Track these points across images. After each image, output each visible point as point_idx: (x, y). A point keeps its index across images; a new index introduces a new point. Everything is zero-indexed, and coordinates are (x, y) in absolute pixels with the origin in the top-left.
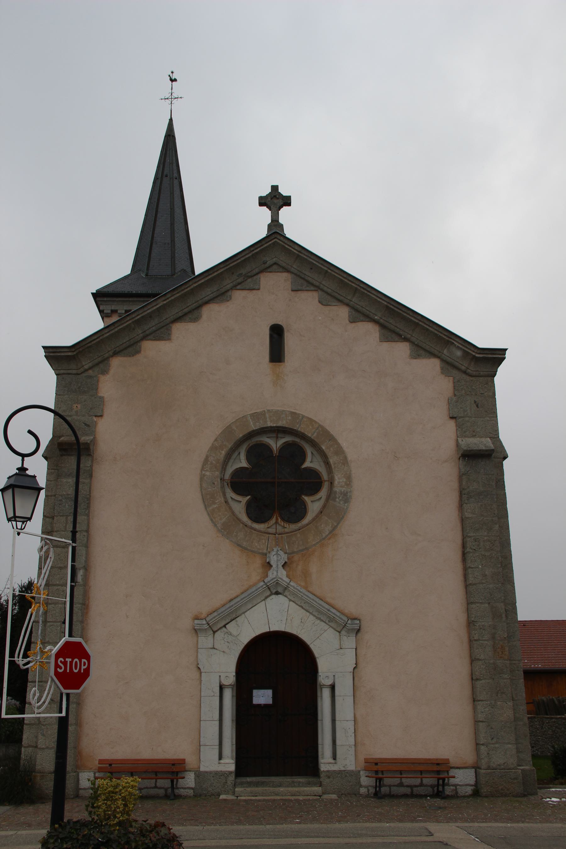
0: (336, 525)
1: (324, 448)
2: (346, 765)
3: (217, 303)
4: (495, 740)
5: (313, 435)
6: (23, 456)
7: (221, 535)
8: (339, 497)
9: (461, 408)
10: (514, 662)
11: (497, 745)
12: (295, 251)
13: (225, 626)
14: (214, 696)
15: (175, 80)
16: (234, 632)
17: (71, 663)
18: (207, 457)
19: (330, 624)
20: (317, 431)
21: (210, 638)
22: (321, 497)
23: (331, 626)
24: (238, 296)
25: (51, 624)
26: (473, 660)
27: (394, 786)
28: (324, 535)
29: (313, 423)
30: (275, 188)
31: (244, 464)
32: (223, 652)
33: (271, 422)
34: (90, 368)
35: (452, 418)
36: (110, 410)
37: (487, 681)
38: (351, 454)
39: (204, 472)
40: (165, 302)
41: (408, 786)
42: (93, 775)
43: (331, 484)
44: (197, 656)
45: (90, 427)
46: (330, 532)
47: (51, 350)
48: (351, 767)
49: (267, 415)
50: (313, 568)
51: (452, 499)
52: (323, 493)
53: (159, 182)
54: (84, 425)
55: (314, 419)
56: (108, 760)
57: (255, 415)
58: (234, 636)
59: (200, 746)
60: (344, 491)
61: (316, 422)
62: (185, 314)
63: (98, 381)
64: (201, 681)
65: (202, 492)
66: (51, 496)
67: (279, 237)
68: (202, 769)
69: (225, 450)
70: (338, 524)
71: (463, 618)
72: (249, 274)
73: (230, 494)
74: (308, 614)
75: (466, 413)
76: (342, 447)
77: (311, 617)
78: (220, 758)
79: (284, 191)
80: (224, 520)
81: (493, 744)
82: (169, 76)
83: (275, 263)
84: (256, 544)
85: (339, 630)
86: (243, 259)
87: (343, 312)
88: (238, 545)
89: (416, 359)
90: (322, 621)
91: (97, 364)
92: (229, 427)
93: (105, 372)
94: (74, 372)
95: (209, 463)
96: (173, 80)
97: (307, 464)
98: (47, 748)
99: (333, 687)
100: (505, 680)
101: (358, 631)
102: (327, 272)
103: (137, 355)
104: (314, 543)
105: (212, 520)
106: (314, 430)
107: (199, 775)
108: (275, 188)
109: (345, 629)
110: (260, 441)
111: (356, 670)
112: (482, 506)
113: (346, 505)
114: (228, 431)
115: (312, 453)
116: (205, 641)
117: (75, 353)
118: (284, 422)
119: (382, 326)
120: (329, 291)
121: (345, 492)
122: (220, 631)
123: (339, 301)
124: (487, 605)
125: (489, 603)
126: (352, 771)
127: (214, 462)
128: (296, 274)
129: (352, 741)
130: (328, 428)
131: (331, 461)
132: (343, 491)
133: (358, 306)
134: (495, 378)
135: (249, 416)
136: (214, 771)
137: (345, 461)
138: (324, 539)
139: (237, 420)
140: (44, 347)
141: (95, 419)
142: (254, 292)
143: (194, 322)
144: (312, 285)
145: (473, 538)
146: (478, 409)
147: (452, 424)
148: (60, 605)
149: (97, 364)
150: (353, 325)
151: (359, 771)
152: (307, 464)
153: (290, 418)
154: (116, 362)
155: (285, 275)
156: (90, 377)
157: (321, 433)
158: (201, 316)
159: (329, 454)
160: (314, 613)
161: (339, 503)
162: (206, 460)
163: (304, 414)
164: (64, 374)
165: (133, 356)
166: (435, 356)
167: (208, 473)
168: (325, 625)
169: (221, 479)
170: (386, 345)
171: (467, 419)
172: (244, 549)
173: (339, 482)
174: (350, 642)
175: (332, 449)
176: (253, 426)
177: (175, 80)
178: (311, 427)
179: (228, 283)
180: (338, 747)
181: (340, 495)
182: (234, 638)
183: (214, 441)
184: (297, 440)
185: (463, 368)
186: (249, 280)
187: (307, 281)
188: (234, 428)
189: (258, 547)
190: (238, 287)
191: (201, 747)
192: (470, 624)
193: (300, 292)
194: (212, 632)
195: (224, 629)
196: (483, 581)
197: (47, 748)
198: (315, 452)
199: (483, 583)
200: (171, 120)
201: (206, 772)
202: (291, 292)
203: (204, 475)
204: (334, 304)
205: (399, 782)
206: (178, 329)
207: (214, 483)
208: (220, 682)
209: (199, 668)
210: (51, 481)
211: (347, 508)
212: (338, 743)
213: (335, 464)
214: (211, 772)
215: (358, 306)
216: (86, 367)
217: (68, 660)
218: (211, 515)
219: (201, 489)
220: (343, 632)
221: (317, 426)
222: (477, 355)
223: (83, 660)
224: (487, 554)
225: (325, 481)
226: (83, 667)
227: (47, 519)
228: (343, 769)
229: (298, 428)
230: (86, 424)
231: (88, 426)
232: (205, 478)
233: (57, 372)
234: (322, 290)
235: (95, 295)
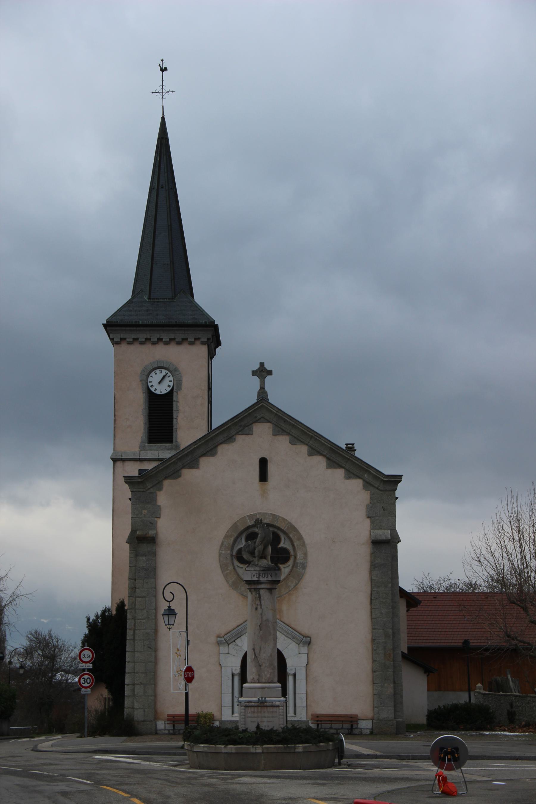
1: (291, 536)
2: (301, 717)
3: (227, 444)
4: (382, 705)
5: (285, 528)
6: (169, 602)
9: (374, 511)
10: (397, 662)
11: (383, 708)
12: (274, 411)
13: (234, 641)
14: (229, 680)
15: (166, 69)
16: (240, 645)
17: (189, 673)
19: (294, 640)
21: (226, 647)
22: (289, 565)
23: (294, 641)
24: (240, 439)
25: (138, 641)
26: (374, 661)
27: (328, 729)
28: (291, 589)
30: (262, 364)
32: (234, 655)
34: (151, 487)
35: (368, 517)
37: (381, 673)
38: (307, 540)
39: (221, 551)
40: (195, 446)
41: (335, 729)
42: (164, 723)
43: (295, 557)
44: (219, 658)
45: (153, 525)
46: (294, 587)
47: (128, 478)
48: (304, 718)
50: (284, 608)
52: (291, 562)
53: (154, 192)
54: (149, 523)
56: (172, 715)
57: (250, 516)
58: (239, 646)
59: (222, 707)
60: (303, 562)
62: (208, 452)
63: (156, 496)
64: (221, 671)
65: (220, 563)
66: (133, 566)
67: (264, 402)
68: (223, 719)
69: (233, 538)
70: (299, 582)
71: (369, 637)
72: (246, 425)
74: (281, 634)
75: (376, 514)
76: (301, 536)
77: (283, 636)
78: (233, 713)
79: (268, 367)
80: (233, 579)
81: (381, 707)
82: (159, 65)
83: (262, 417)
85: (298, 643)
86: (242, 417)
87: (304, 449)
88: (242, 595)
89: (348, 479)
90: (289, 638)
91: (156, 485)
92: (235, 523)
93: (160, 489)
94: (142, 490)
95: (224, 546)
96: (164, 70)
97: (281, 545)
98: (140, 708)
99: (294, 675)
100: (390, 673)
101: (309, 644)
102: (294, 425)
103: (179, 478)
104: (285, 593)
105: (226, 580)
107: (221, 722)
108: (262, 364)
109: (301, 642)
110: (254, 531)
111: (307, 666)
112: (382, 572)
113: (304, 570)
114: (235, 526)
115: (284, 538)
116: (224, 649)
117: (142, 480)
118: (268, 520)
119: (328, 459)
120: (296, 436)
121: (303, 563)
122: (231, 644)
123: (302, 442)
124: (382, 630)
125: (383, 629)
126: (305, 721)
127: (227, 545)
128: (275, 425)
129: (304, 704)
130: (294, 524)
131: (295, 544)
132: (302, 562)
133: (313, 446)
134: (396, 492)
135: (247, 516)
136: (230, 720)
137: (304, 544)
139: (240, 519)
140: (123, 477)
141: (156, 519)
142: (250, 436)
143: (213, 456)
144: (286, 432)
145: (376, 591)
146: (384, 512)
147: (368, 521)
148: (142, 631)
149: (156, 485)
150: (310, 457)
151: (308, 721)
152: (281, 545)
153: (271, 518)
154: (166, 483)
155: (269, 424)
156: (152, 493)
158: (217, 453)
159: (294, 540)
160: (284, 634)
161: (300, 569)
162: (222, 544)
163: (279, 515)
164: (136, 491)
165: (177, 479)
166: (360, 478)
167: (223, 552)
168: (291, 640)
169: (231, 555)
170: (330, 471)
171: (377, 518)
173: (299, 557)
174: (304, 650)
175: (296, 537)
177: (166, 69)
178: (283, 523)
180: (297, 708)
182: (240, 648)
183: (227, 532)
184: (276, 530)
185: (376, 486)
186: (247, 428)
187: (283, 430)
188: (238, 524)
190: (240, 433)
191: (222, 707)
192: (373, 641)
193: (277, 436)
194: (227, 644)
195: (234, 643)
196: (381, 617)
197: (140, 708)
198: (286, 538)
199: (380, 618)
200: (163, 119)
201: (225, 721)
202: (272, 436)
203: (221, 553)
204: (299, 444)
205: (330, 727)
206: (204, 462)
207: (227, 558)
208: (232, 672)
209: (220, 665)
210: (132, 558)
211: (304, 573)
212: (297, 705)
213: (297, 546)
214: (228, 721)
215: (313, 446)
216: (149, 487)
217: (188, 673)
218: (226, 576)
219: (220, 562)
220: (301, 645)
222: (385, 479)
223: (192, 673)
224: (384, 601)
225: (292, 556)
226: (192, 675)
227: (131, 580)
228: (300, 719)
230: (151, 523)
231: (152, 524)
233: (132, 490)
234: (292, 435)
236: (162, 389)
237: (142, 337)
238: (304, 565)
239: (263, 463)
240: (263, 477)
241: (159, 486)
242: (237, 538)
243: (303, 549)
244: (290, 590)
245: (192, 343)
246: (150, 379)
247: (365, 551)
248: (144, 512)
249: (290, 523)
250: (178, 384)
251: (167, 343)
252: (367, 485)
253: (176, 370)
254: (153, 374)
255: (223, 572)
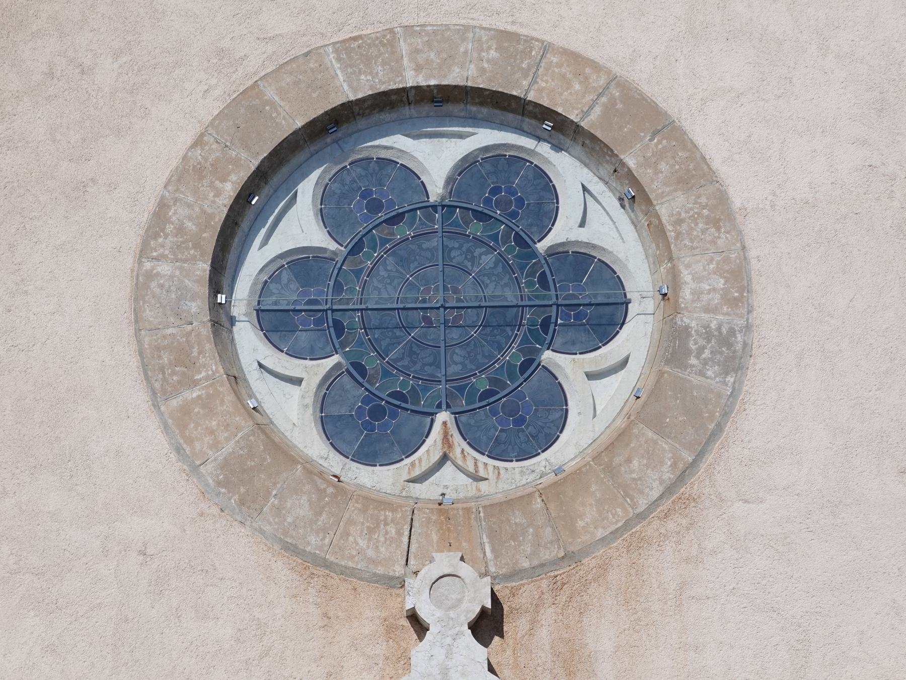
0: (690, 459)
5: (586, 114)
7: (215, 510)
8: (701, 350)
18: (162, 206)
20: (604, 99)
22: (624, 363)
28: (643, 504)
29: (588, 71)
33: (418, 69)
39: (148, 265)
46: (669, 490)
49: (404, 47)
55: (591, 54)
57: (354, 45)
60: (719, 328)
61: (596, 67)
65: (139, 342)
69: (234, 177)
70: (700, 457)
80: (229, 447)
84: (362, 543)
88: (291, 549)
95: (170, 228)
104: (600, 533)
105: (178, 450)
106: (590, 97)
113: (730, 379)
118: (472, 70)
121: (724, 331)
127: (189, 225)
130: (647, 89)
132: (713, 325)
135: (330, 49)
138: (642, 517)
139: (282, 66)
153: (493, 54)
157: (619, 106)
163: (546, 38)
173: (697, 294)
178: (577, 87)
181: (701, 342)
188: (271, 93)
189: (370, 553)
203: (150, 276)
211: (734, 394)
219: (138, 331)
221: (602, 81)
229: (527, 92)
232: (153, 284)
238: (730, 346)
243: (720, 242)
244: (640, 510)
249: (626, 87)
255: (156, 398)
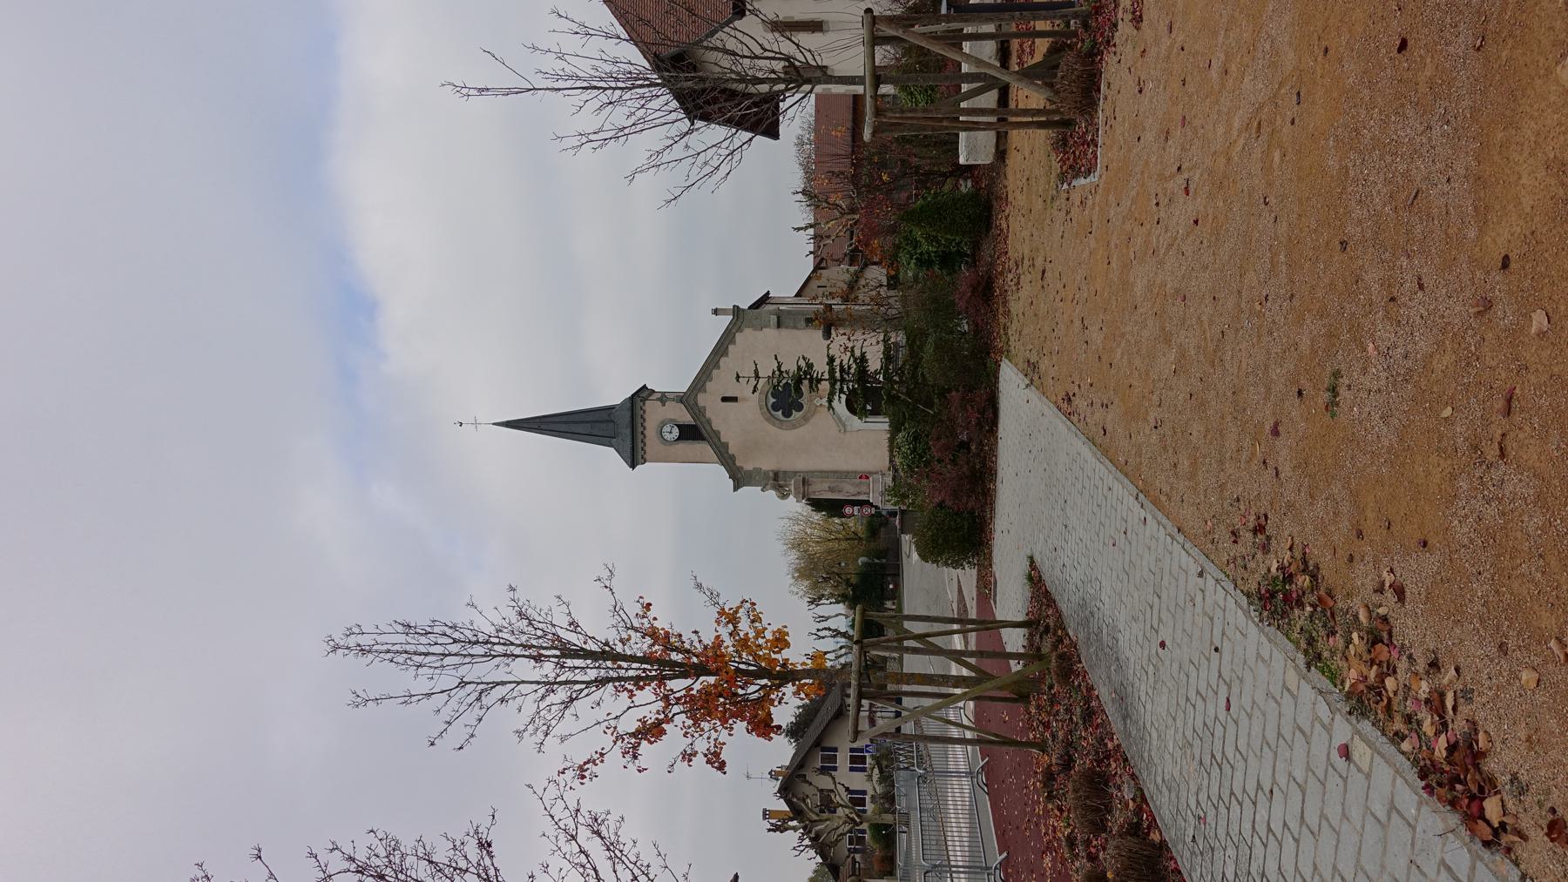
24: (708, 415)
31: (780, 412)
36: (758, 465)
45: (766, 473)
51: (795, 331)
73: (792, 418)
93: (742, 468)
114: (767, 420)
116: (848, 428)
147: (764, 330)
154: (738, 464)
170: (730, 354)
172: (813, 415)
176: (765, 409)
179: (703, 420)
200: (494, 424)
235: (633, 466)
236: (676, 432)
237: (640, 445)
239: (725, 399)
240: (734, 399)
241: (740, 469)
242: (774, 417)
245: (644, 411)
246: (669, 439)
247: (784, 332)
248: (757, 478)
250: (671, 420)
251: (645, 429)
252: (740, 330)
253: (662, 422)
254: (665, 438)
